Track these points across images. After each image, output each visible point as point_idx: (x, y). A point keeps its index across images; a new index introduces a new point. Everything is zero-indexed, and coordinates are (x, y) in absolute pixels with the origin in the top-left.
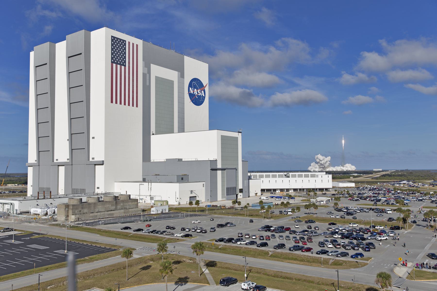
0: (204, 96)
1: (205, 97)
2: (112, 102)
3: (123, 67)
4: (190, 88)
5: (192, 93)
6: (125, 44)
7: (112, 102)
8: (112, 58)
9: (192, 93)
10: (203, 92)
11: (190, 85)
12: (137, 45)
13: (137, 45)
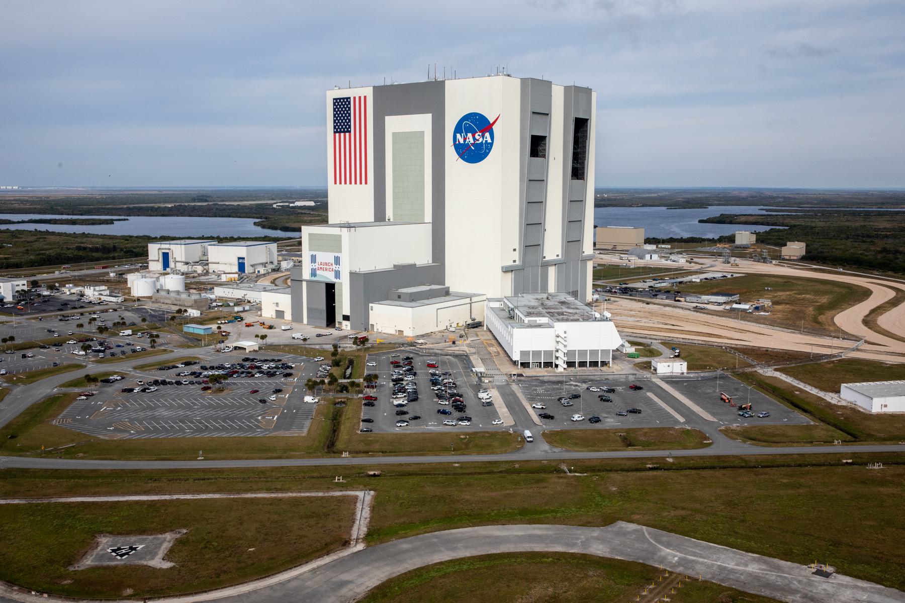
0: (489, 141)
1: (492, 144)
2: (335, 183)
3: (347, 134)
4: (458, 135)
5: (462, 141)
6: (349, 103)
7: (335, 183)
8: (335, 127)
9: (462, 141)
10: (487, 135)
11: (458, 129)
12: (365, 97)
13: (365, 97)
